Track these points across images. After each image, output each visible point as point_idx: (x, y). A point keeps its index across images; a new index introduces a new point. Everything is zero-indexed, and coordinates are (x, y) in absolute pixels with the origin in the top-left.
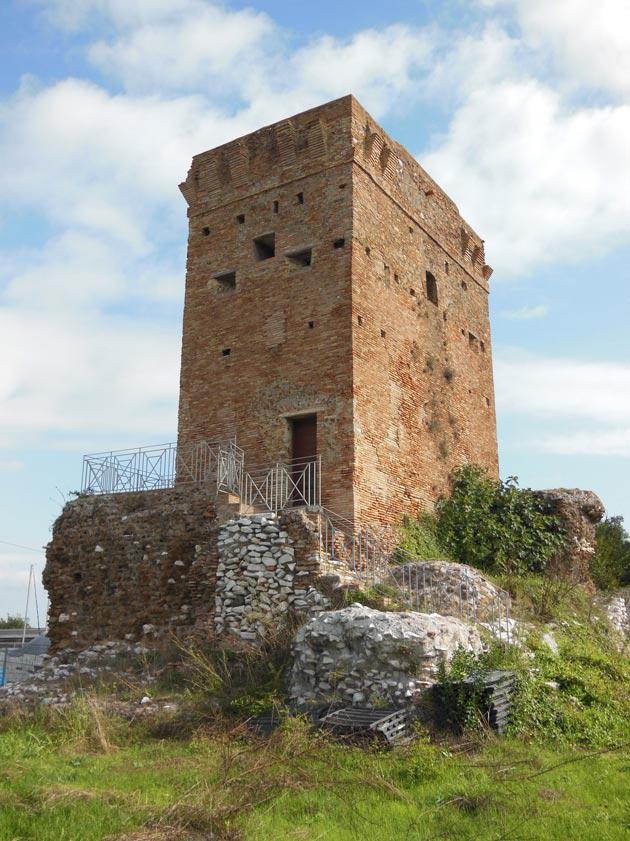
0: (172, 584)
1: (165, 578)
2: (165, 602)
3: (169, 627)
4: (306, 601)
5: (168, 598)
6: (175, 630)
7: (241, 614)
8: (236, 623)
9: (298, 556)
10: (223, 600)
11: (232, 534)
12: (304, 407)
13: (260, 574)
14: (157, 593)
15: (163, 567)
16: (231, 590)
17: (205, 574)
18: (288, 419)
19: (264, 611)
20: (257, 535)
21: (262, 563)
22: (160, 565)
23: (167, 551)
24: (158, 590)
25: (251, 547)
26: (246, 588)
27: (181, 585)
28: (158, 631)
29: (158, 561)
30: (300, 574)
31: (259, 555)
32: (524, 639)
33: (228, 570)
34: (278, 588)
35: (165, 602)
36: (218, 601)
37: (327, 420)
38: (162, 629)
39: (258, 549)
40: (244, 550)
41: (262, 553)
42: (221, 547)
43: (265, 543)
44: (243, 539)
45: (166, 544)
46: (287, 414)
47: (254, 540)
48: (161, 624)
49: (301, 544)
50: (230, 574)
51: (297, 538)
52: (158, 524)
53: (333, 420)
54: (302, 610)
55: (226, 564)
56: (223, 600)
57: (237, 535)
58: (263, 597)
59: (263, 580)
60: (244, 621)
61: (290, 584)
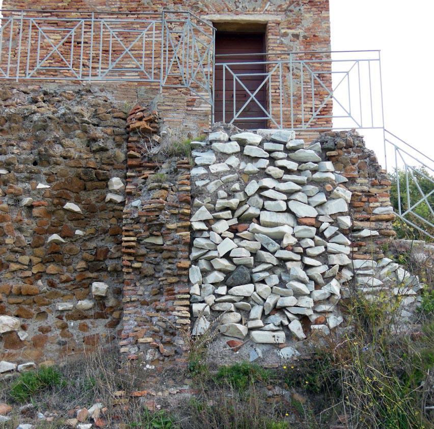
0: (57, 243)
1: (40, 234)
2: (40, 275)
3: (52, 320)
4: (380, 278)
5: (52, 268)
6: (64, 327)
7: (246, 299)
8: (238, 316)
9: (357, 204)
10: (205, 273)
11: (222, 156)
12: (245, 11)
13: (287, 229)
14: (25, 259)
15: (36, 212)
16: (227, 256)
17: (162, 225)
18: (215, 24)
19: (298, 294)
20: (280, 163)
21: (288, 211)
22: (30, 207)
23: (49, 182)
24: (23, 254)
25: (266, 182)
26: (253, 254)
27: (77, 247)
28: (24, 328)
29: (26, 200)
30: (366, 233)
31: (285, 197)
32: (389, 309)
33: (217, 219)
34: (324, 257)
35: (40, 275)
36: (195, 275)
37: (285, 35)
38: (34, 325)
39: (283, 186)
40: (252, 187)
41: (290, 193)
42: (202, 178)
43: (295, 177)
44: (251, 167)
45: (45, 170)
46: (217, 17)
47: (272, 170)
48: (29, 316)
49: (363, 184)
50: (222, 226)
51: (356, 174)
52: (23, 134)
53: (296, 36)
54: (373, 293)
55: (212, 211)
56: (205, 273)
57: (233, 161)
58: (296, 269)
59: (293, 241)
60: (256, 312)
61: (348, 250)
